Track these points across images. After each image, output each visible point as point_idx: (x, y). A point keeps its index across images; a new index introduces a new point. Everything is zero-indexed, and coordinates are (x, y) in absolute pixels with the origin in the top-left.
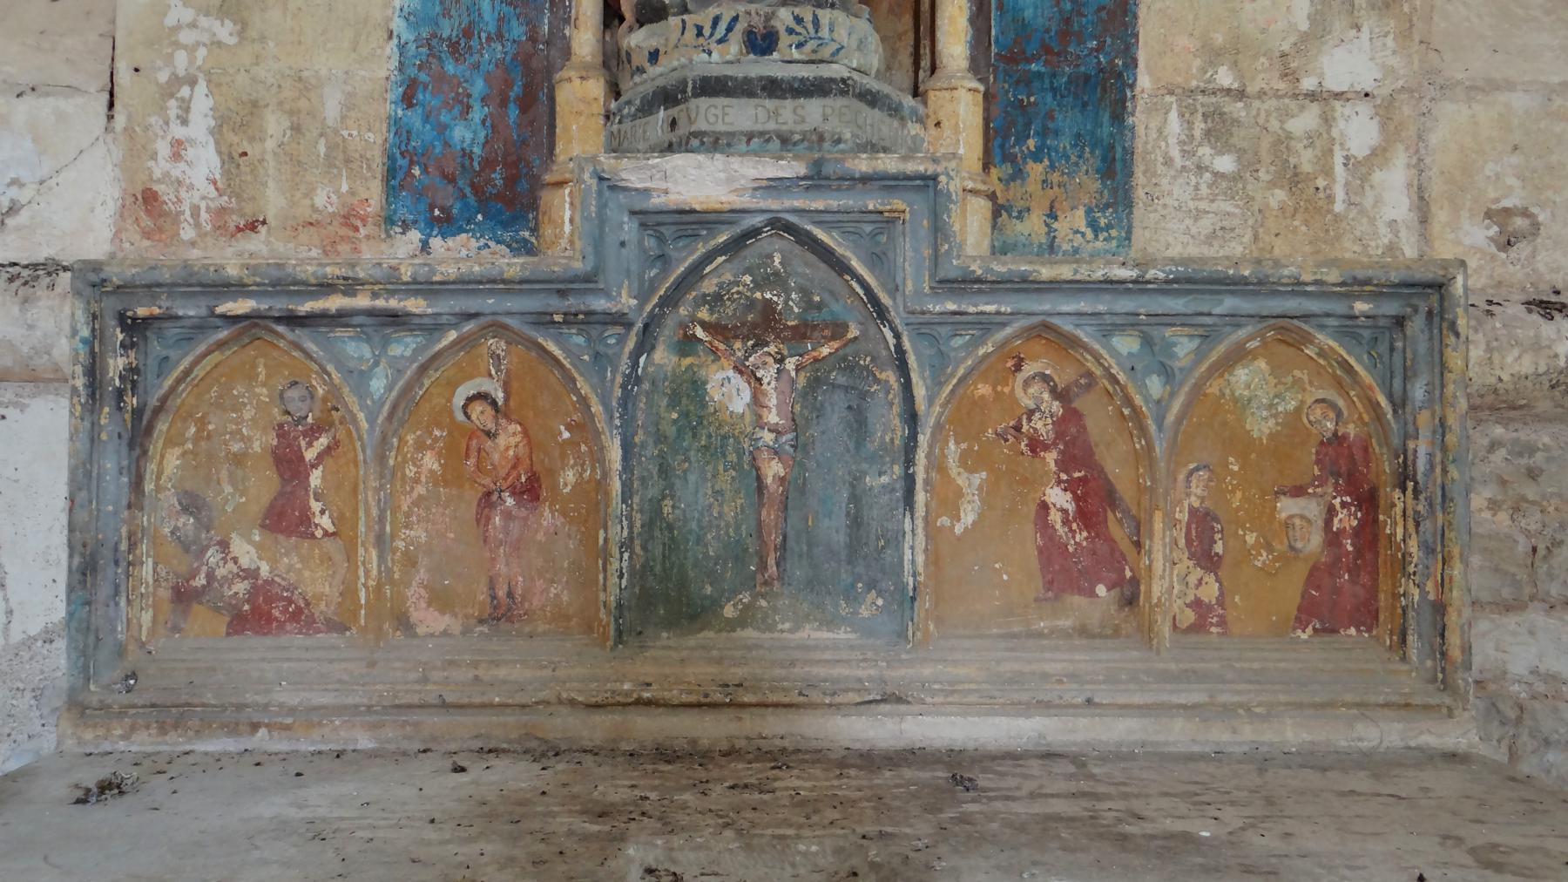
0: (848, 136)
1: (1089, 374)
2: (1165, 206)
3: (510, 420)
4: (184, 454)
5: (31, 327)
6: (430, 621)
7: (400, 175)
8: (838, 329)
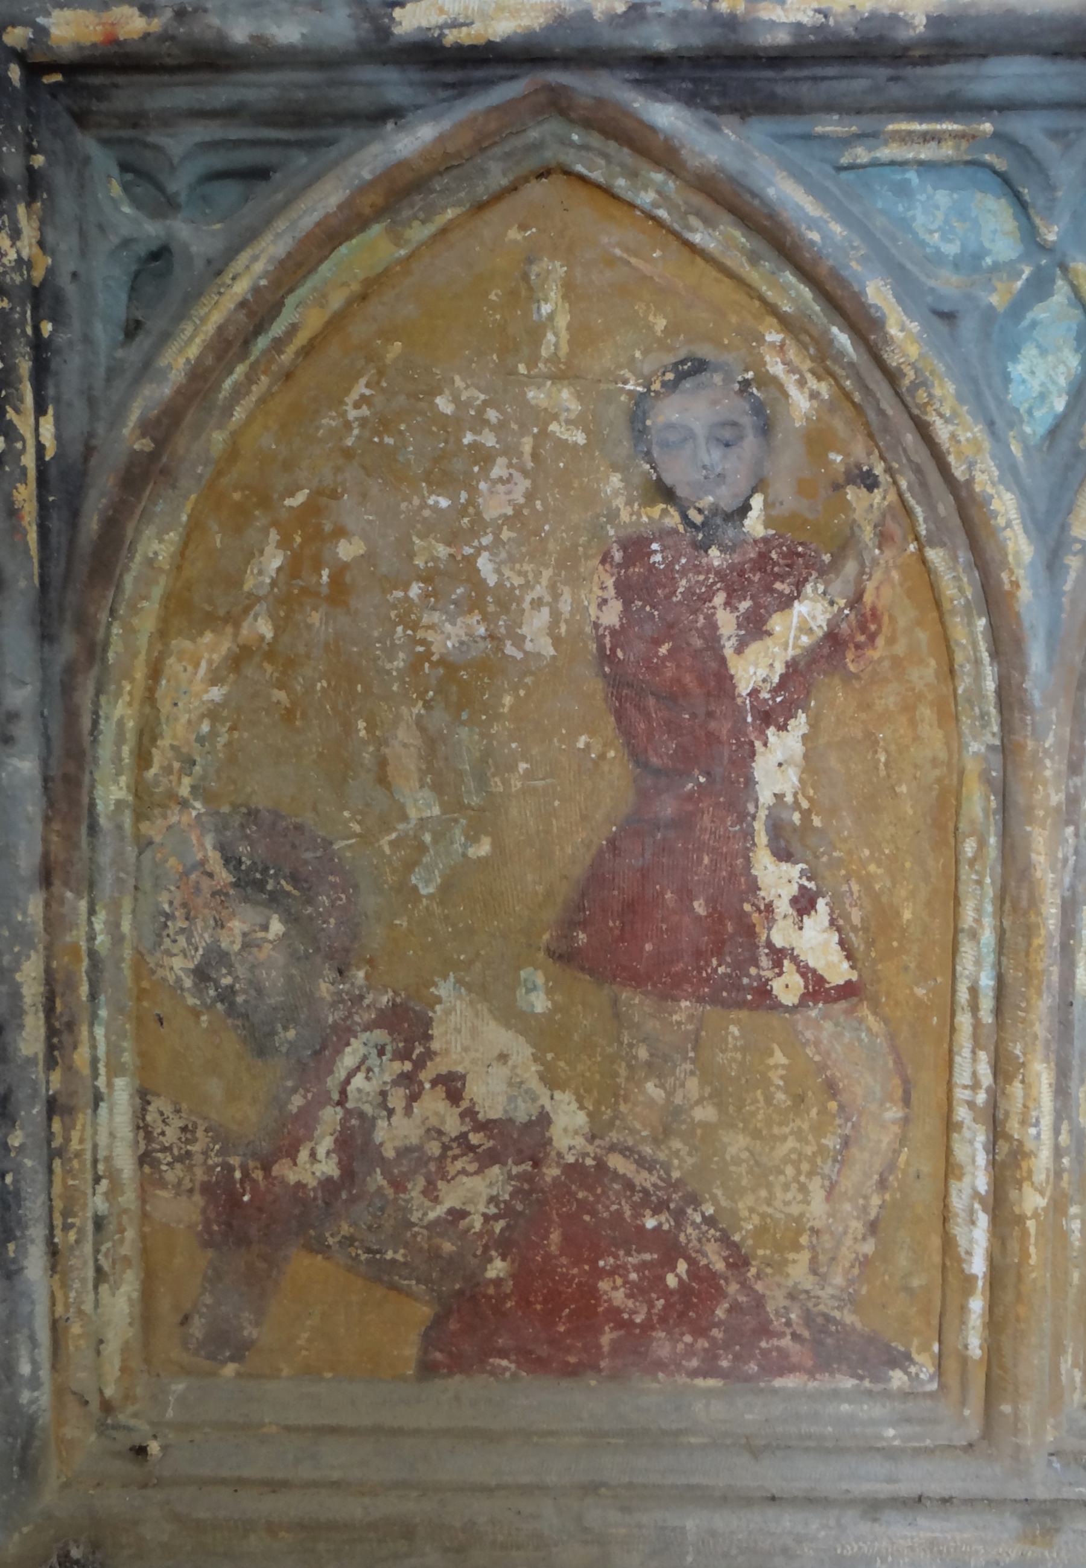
4: (239, 659)
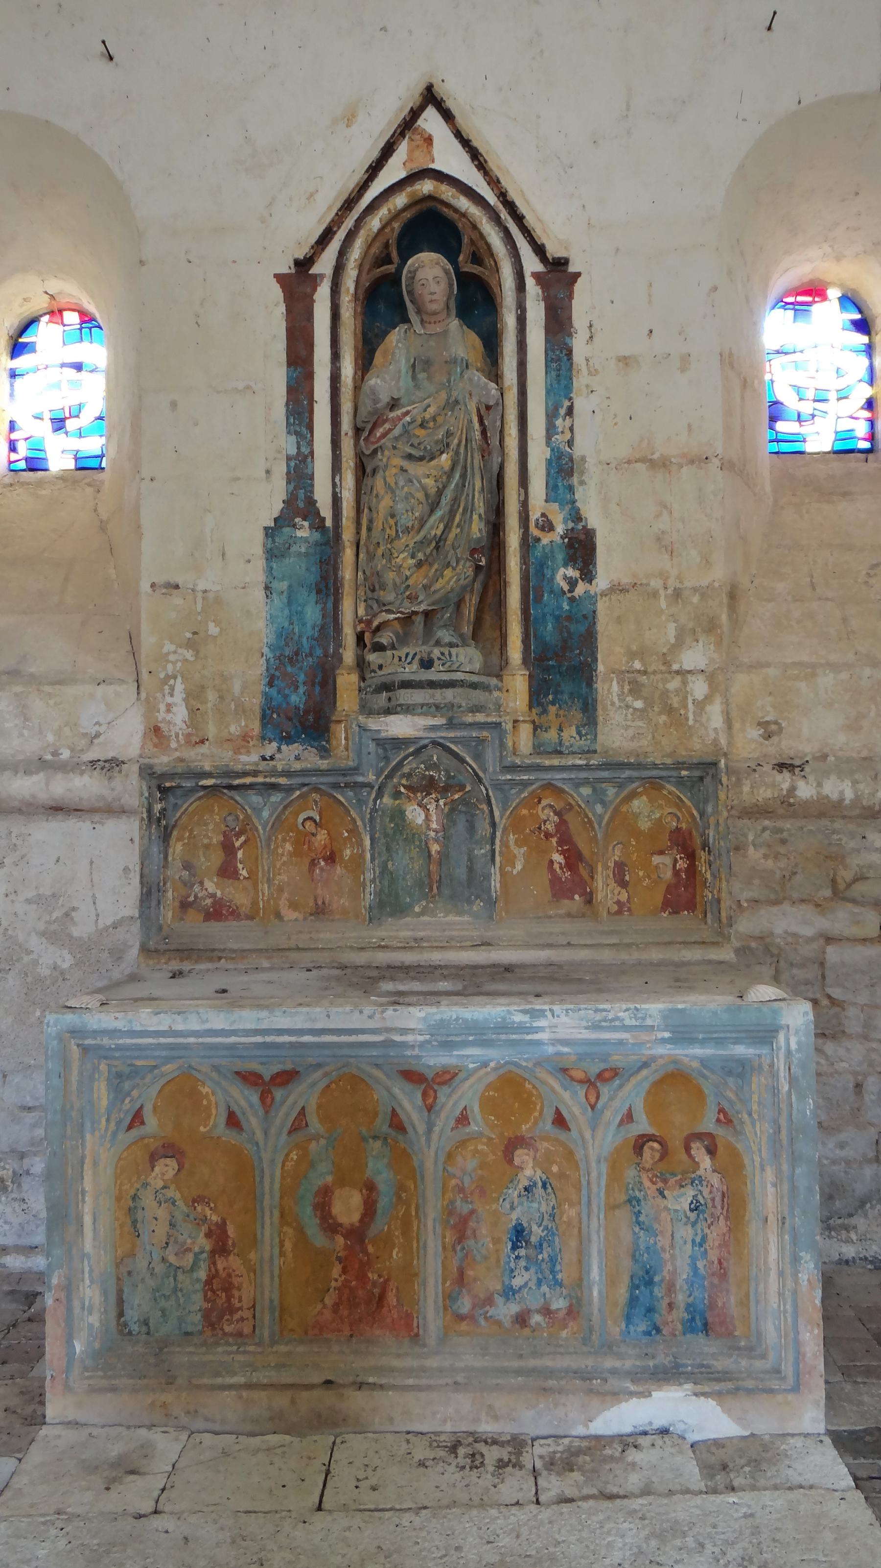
0: (464, 704)
1: (570, 804)
2: (612, 724)
3: (322, 829)
5: (113, 790)
6: (290, 915)
7: (268, 718)
8: (462, 787)
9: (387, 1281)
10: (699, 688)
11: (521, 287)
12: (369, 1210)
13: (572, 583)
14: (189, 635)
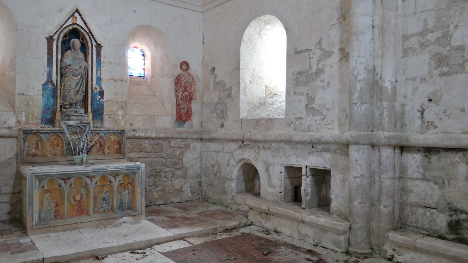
9: (84, 208)
10: (120, 118)
11: (92, 47)
12: (81, 197)
13: (100, 99)
14: (26, 104)
